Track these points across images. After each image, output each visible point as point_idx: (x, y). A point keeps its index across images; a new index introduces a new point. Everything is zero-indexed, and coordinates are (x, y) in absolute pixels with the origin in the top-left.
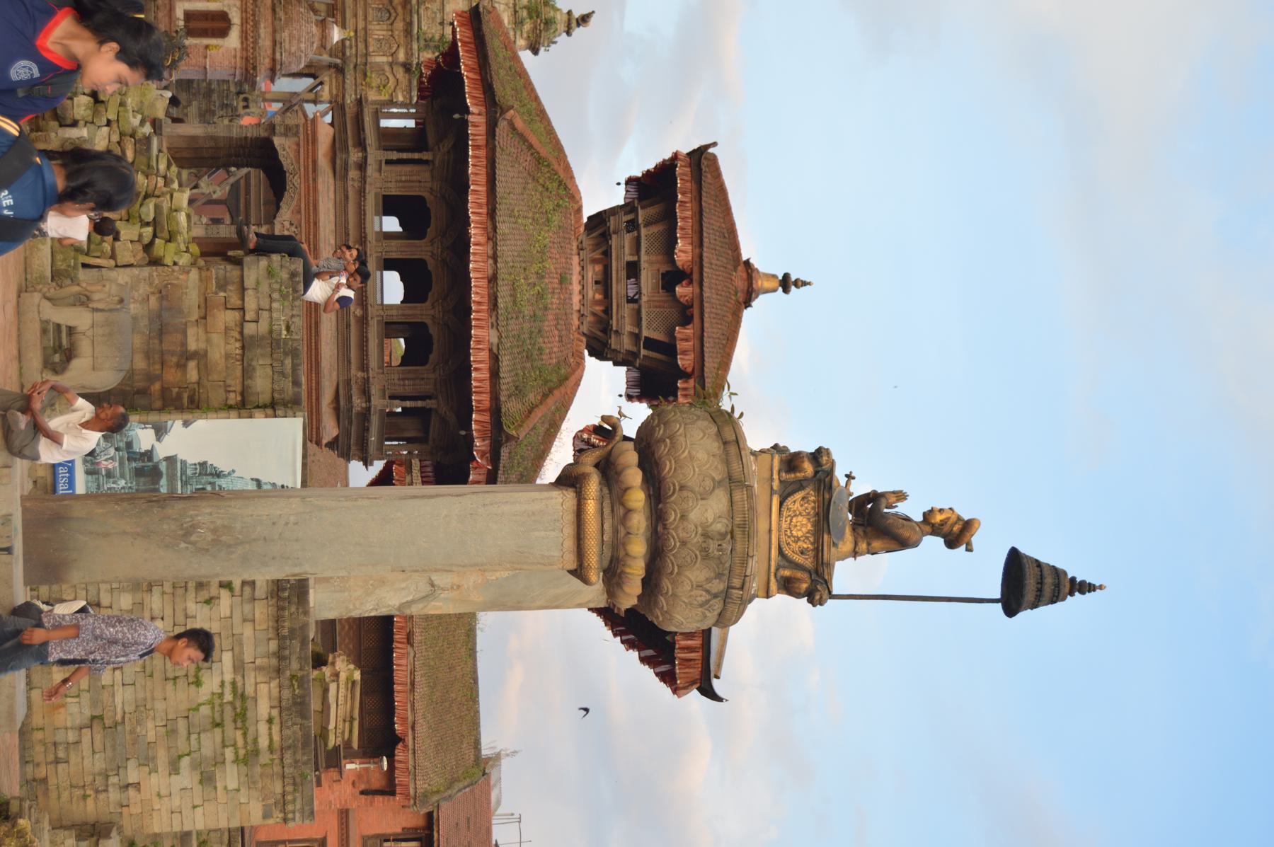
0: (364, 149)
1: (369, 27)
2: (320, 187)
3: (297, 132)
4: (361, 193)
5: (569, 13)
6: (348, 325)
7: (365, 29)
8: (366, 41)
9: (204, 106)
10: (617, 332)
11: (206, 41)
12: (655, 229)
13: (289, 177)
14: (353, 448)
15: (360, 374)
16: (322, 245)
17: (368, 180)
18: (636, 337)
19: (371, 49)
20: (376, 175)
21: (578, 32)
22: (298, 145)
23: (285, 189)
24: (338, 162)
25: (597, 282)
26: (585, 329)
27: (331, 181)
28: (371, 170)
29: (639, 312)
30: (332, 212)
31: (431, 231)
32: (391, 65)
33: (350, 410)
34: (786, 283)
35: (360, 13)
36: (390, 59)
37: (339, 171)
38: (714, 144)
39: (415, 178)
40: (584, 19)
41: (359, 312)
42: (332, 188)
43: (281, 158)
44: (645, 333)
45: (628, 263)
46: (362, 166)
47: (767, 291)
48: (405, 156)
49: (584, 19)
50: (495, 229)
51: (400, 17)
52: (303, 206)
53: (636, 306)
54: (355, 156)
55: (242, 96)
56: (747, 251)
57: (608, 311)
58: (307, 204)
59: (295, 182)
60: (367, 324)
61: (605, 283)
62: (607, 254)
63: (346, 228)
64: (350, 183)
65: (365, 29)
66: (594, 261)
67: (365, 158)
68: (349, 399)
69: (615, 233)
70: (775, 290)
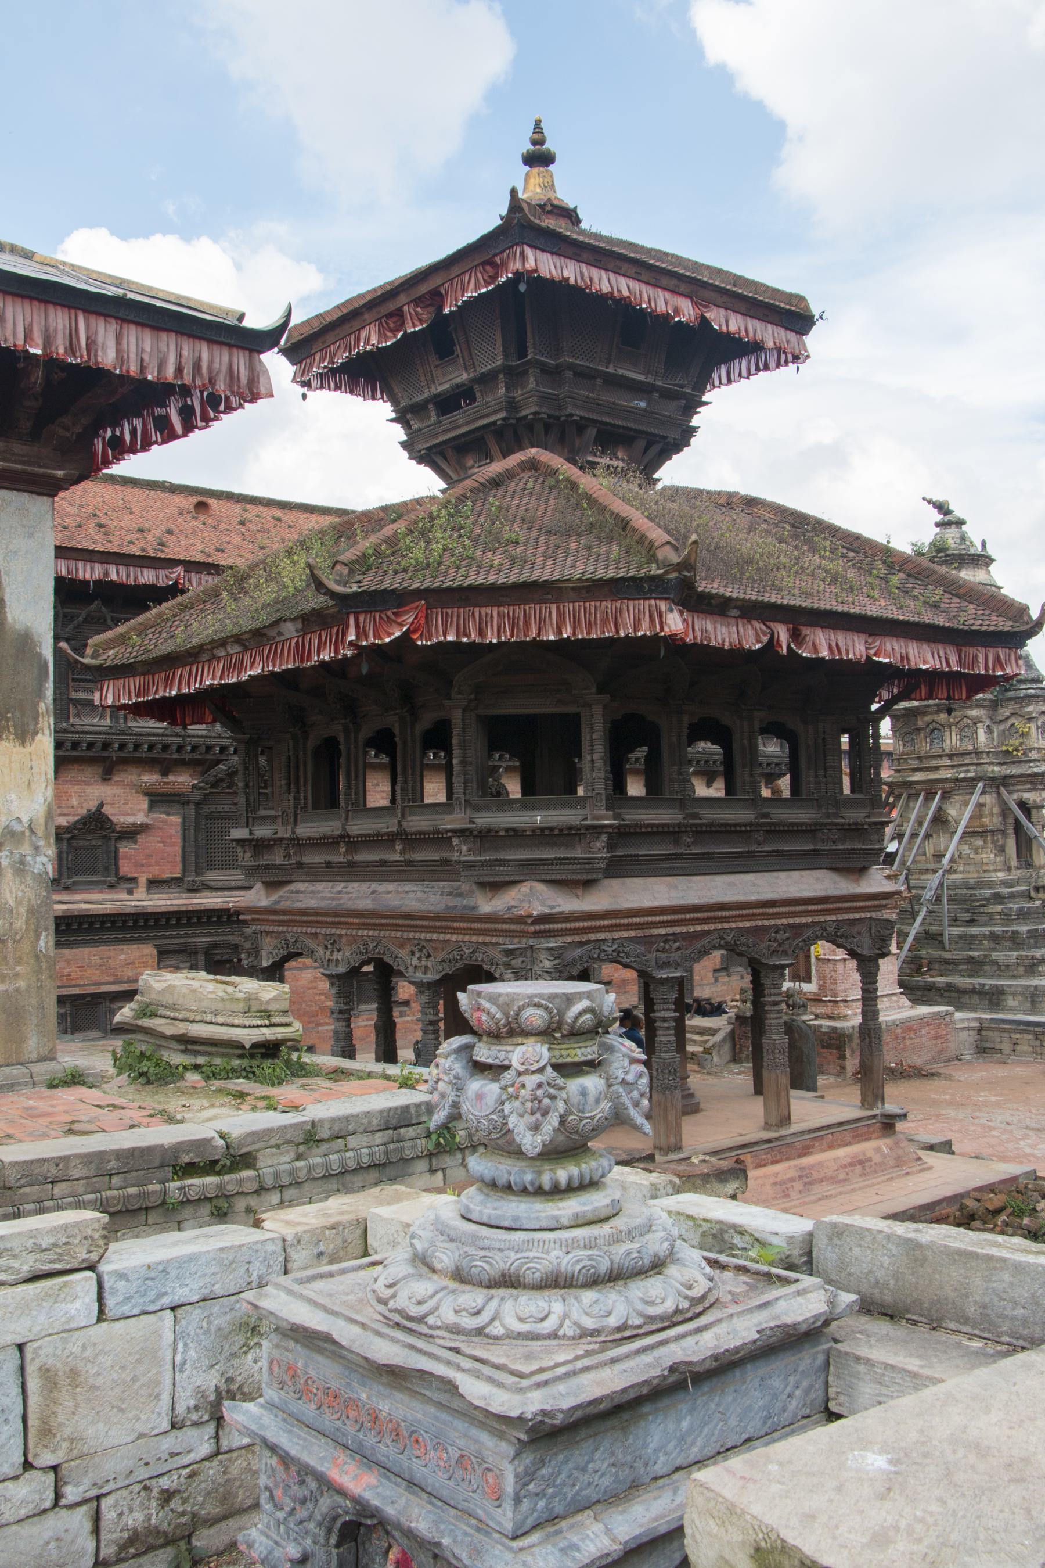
1: (947, 751)
4: (297, 843)
5: (937, 525)
7: (950, 756)
8: (963, 754)
9: (1008, 944)
11: (813, 960)
14: (578, 853)
18: (514, 375)
19: (971, 748)
21: (959, 511)
22: (267, 933)
27: (292, 887)
28: (263, 832)
35: (934, 763)
40: (941, 507)
49: (941, 507)
51: (935, 717)
53: (476, 387)
55: (1033, 894)
65: (950, 756)
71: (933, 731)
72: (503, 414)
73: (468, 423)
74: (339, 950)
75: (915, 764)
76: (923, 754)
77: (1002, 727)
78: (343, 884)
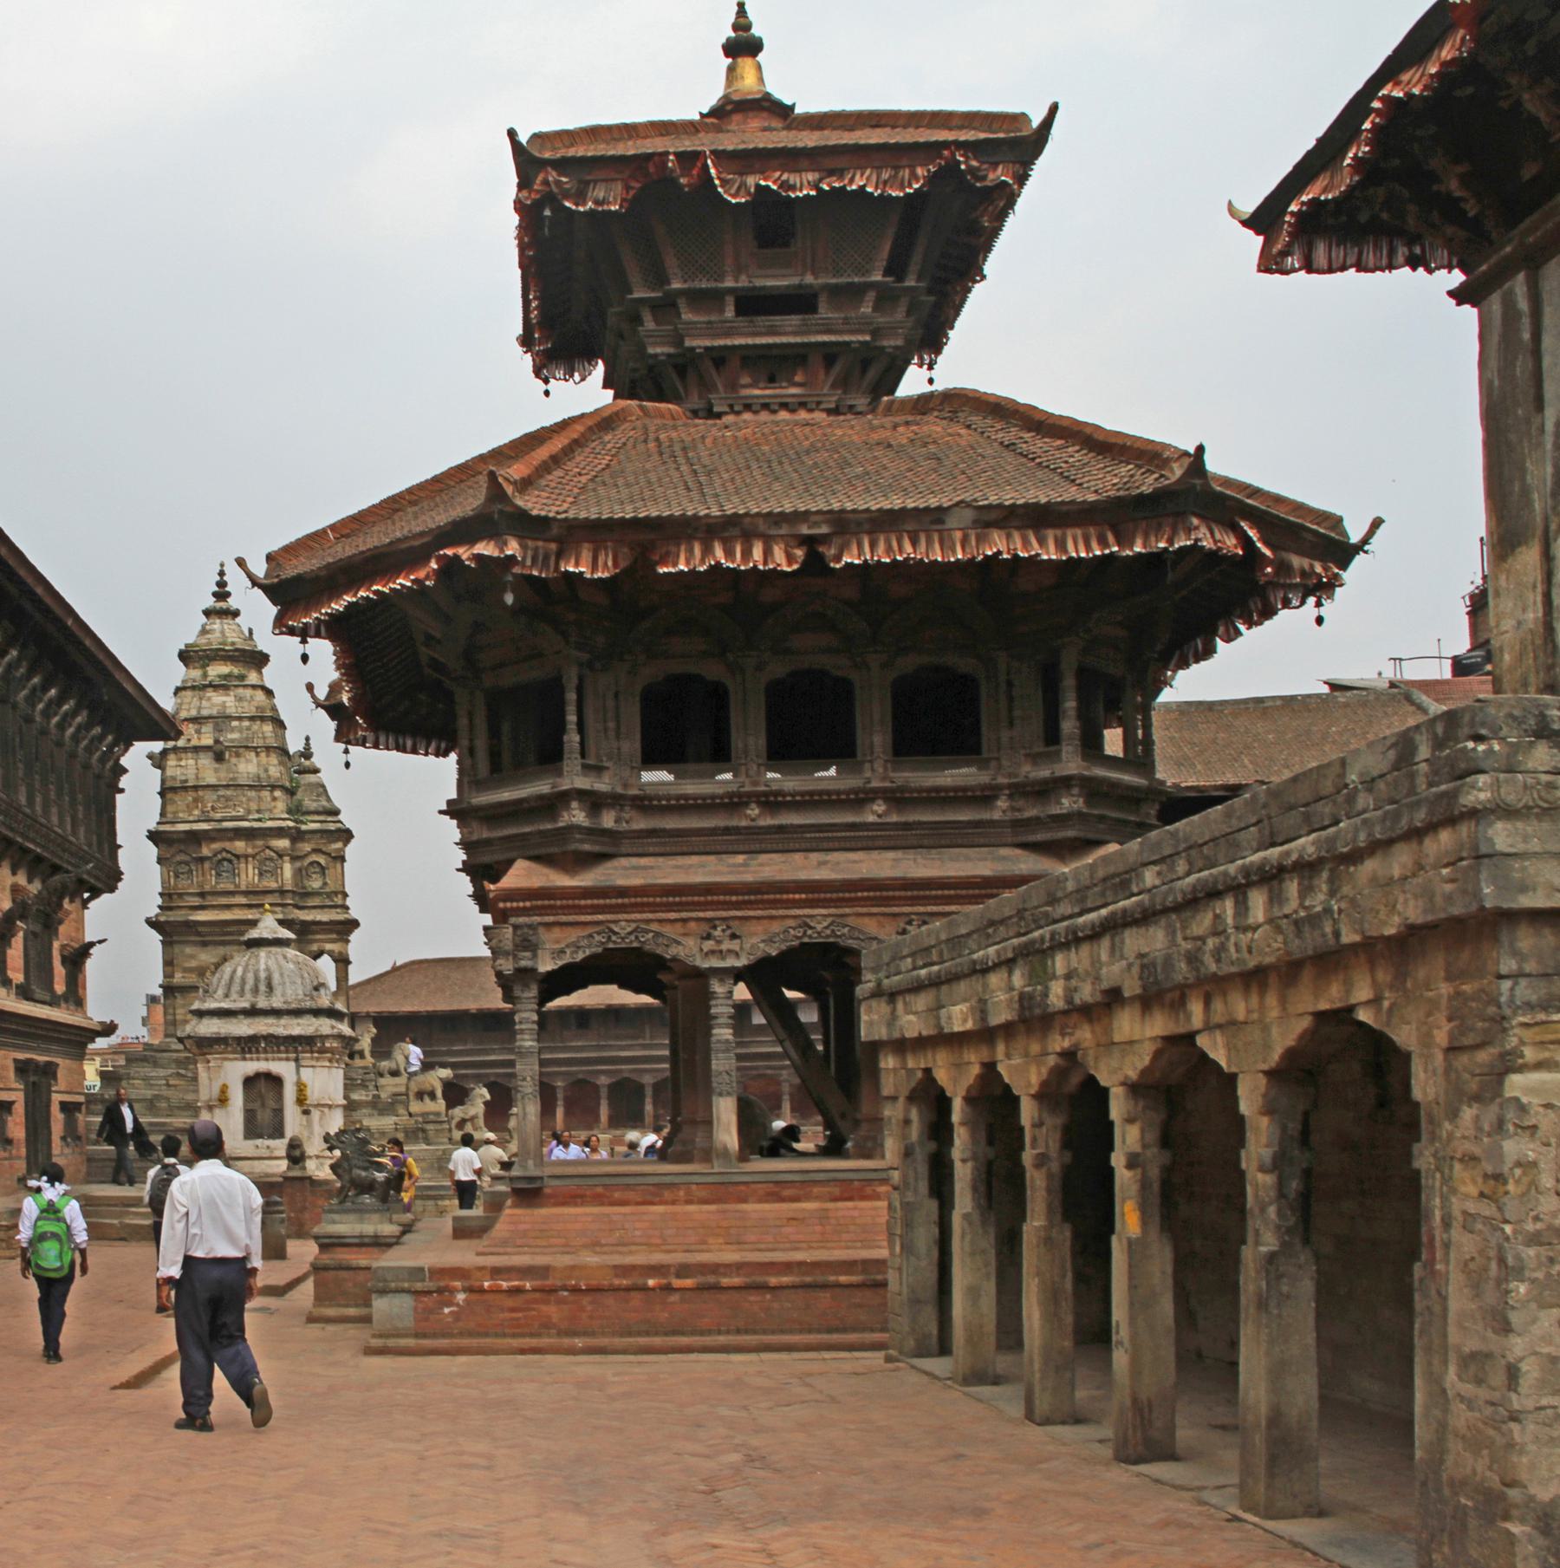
2: (636, 881)
3: (530, 926)
6: (906, 826)
10: (876, 333)
12: (671, 263)
13: (615, 943)
16: (748, 878)
17: (619, 790)
20: (606, 777)
23: (638, 952)
24: (587, 847)
25: (772, 379)
26: (861, 402)
28: (602, 785)
29: (836, 292)
30: (681, 860)
31: (713, 671)
32: (294, 859)
33: (1080, 815)
36: (287, 858)
37: (608, 847)
38: (512, 134)
39: (610, 703)
41: (879, 807)
42: (634, 861)
43: (580, 956)
46: (595, 803)
47: (761, 80)
48: (572, 718)
50: (733, 521)
52: (673, 915)
54: (577, 815)
56: (690, 111)
57: (830, 355)
58: (669, 907)
59: (625, 929)
60: (902, 789)
61: (773, 364)
62: (719, 358)
63: (713, 832)
64: (624, 826)
66: (733, 386)
67: (581, 794)
68: (1062, 820)
69: (682, 342)
70: (759, 67)
71: (220, 861)
73: (795, 334)
74: (734, 936)
75: (196, 901)
76: (207, 888)
77: (298, 864)
78: (740, 858)
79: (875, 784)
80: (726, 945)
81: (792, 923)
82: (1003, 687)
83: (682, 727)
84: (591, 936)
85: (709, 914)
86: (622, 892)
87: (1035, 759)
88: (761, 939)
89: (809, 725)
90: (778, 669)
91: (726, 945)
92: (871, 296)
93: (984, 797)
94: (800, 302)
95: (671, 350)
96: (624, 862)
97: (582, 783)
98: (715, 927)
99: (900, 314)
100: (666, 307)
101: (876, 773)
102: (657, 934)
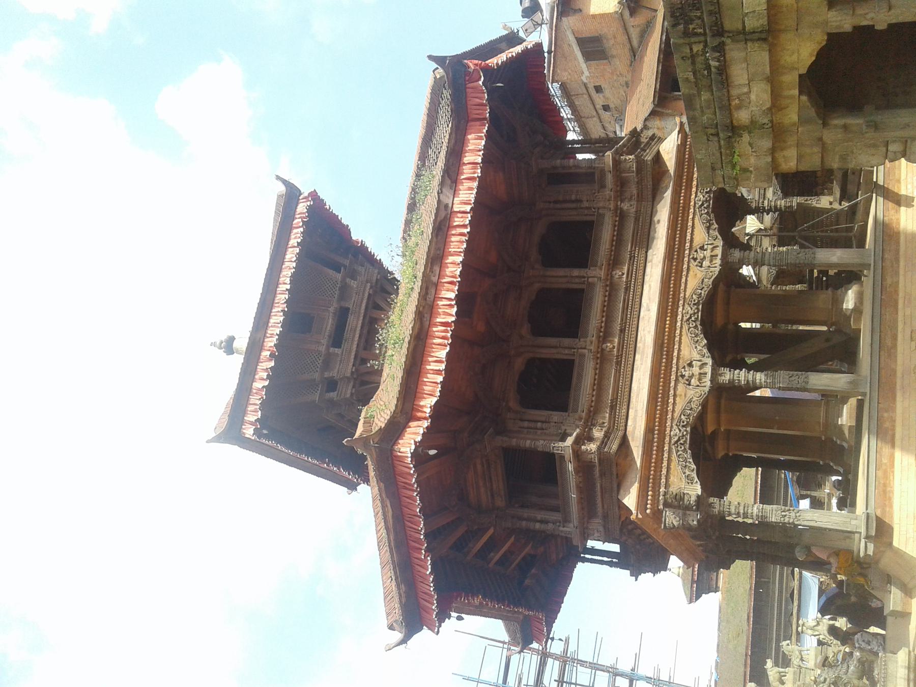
0: (578, 454)
15: (625, 206)
31: (519, 364)
34: (228, 346)
39: (526, 424)
44: (339, 276)
45: (340, 347)
63: (618, 371)
72: (369, 285)
74: (690, 365)
79: (603, 274)
80: (696, 370)
81: (685, 327)
82: (558, 206)
83: (551, 387)
84: (679, 456)
85: (673, 377)
86: (649, 430)
87: (603, 186)
88: (692, 349)
89: (564, 313)
90: (525, 330)
91: (696, 370)
92: (348, 280)
93: (621, 216)
94: (343, 315)
95: (351, 384)
96: (629, 428)
97: (570, 441)
98: (683, 376)
99: (360, 269)
100: (332, 385)
101: (597, 273)
102: (683, 412)
